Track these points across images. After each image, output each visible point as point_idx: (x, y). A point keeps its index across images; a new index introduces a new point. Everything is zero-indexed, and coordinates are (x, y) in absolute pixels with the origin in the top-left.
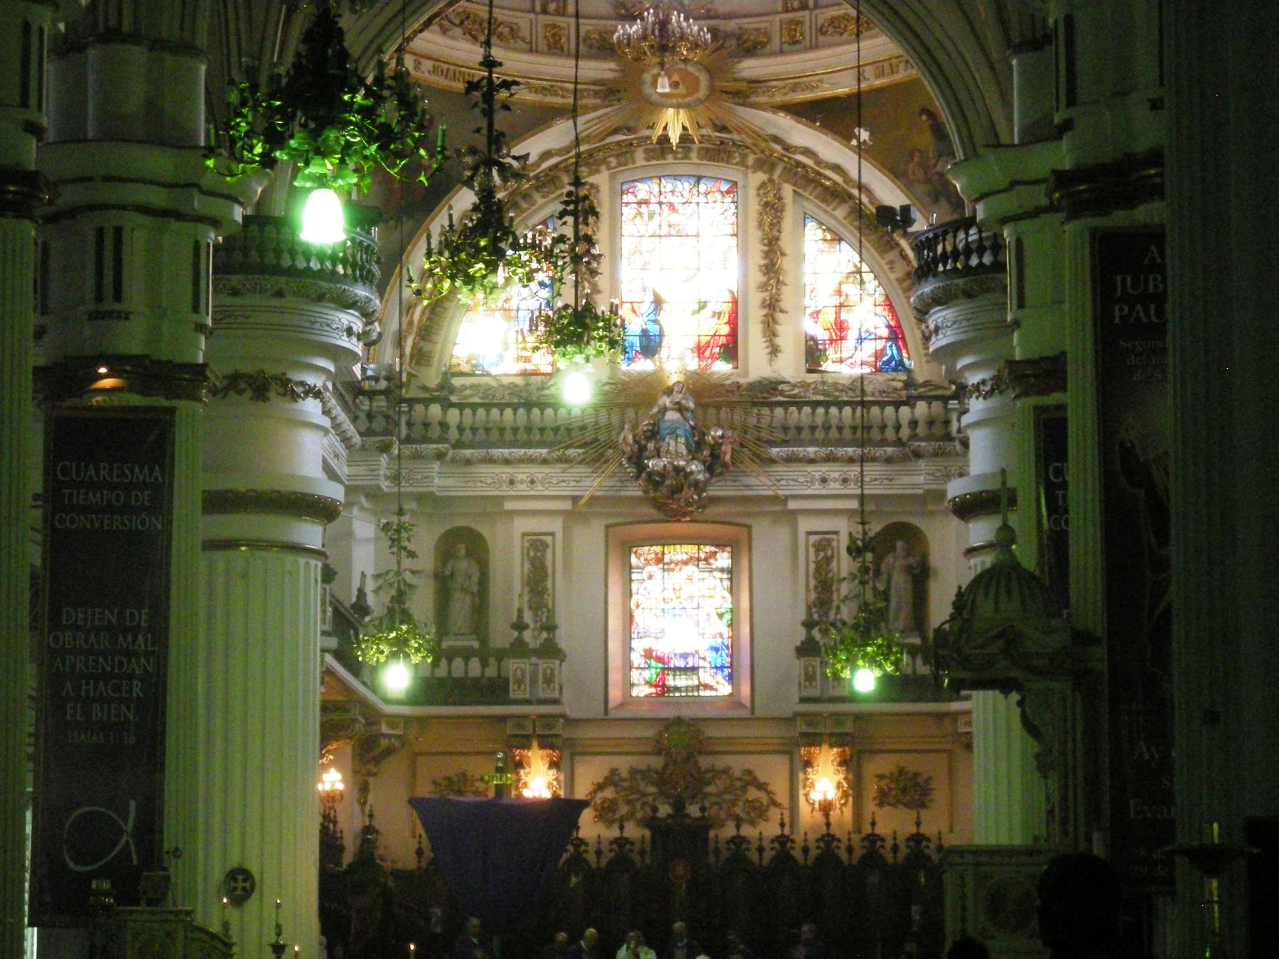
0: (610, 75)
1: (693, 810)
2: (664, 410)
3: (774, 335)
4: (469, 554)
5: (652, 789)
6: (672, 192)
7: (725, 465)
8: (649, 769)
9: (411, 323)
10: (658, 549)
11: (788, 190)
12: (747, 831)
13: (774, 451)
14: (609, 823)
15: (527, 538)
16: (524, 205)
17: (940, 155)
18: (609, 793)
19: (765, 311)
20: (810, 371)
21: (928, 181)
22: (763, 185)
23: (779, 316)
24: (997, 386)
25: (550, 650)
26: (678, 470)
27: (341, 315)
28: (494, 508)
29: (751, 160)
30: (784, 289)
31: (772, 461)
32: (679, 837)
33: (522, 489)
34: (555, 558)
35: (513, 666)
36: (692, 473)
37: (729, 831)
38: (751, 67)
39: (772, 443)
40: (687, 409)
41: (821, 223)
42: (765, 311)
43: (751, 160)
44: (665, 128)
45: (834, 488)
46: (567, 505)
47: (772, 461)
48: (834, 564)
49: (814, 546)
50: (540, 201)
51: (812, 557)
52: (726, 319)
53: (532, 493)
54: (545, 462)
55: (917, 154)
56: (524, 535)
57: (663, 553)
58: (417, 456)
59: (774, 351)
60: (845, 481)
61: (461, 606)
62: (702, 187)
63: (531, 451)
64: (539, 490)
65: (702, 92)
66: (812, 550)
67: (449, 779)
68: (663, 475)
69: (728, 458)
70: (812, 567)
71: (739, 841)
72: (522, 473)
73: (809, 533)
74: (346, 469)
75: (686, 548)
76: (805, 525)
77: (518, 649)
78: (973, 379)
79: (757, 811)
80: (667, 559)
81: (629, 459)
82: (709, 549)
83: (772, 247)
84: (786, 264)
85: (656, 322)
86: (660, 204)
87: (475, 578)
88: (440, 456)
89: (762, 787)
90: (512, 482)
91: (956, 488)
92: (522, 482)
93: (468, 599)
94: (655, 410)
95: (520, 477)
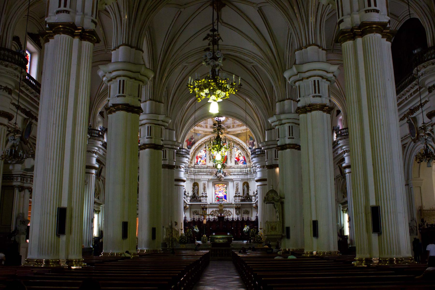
1: (223, 215)
12: (229, 217)
24: (261, 167)
25: (206, 197)
28: (199, 180)
32: (221, 218)
33: (203, 178)
34: (206, 186)
35: (202, 198)
37: (227, 217)
38: (229, 130)
45: (238, 178)
59: (231, 162)
71: (228, 218)
72: (203, 176)
76: (235, 182)
77: (203, 197)
78: (258, 166)
79: (230, 215)
84: (233, 152)
91: (256, 179)
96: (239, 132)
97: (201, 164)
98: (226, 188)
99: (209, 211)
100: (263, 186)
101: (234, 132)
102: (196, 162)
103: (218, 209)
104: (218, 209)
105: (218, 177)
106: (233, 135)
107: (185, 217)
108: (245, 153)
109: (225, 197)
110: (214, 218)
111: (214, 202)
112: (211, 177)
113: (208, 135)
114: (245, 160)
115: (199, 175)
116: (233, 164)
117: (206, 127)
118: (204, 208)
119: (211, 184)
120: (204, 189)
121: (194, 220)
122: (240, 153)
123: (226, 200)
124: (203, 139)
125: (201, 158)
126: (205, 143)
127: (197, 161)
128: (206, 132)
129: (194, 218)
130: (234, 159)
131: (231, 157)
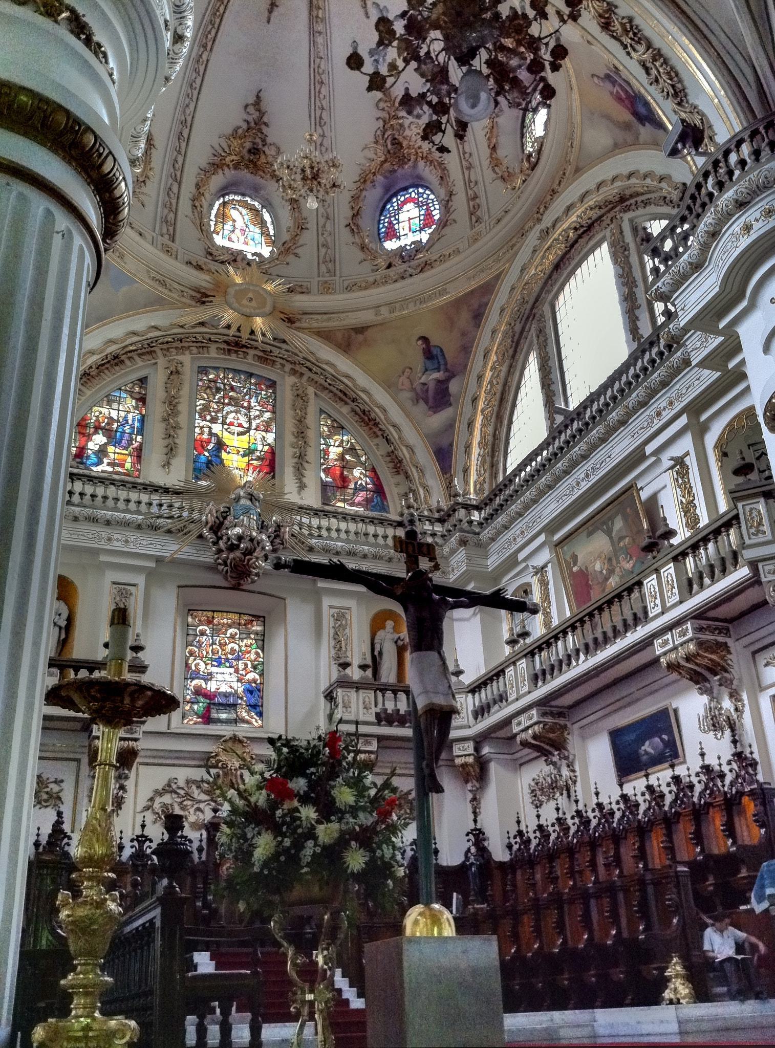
0: (204, 284)
2: (238, 499)
5: (203, 797)
6: (233, 379)
10: (210, 614)
15: (115, 586)
17: (426, 370)
19: (296, 460)
20: (324, 504)
21: (414, 390)
23: (306, 465)
33: (118, 545)
41: (330, 416)
42: (296, 460)
44: (239, 330)
46: (153, 565)
48: (347, 631)
49: (333, 616)
51: (332, 625)
52: (267, 463)
53: (125, 549)
54: (139, 527)
55: (407, 370)
56: (114, 583)
57: (213, 617)
59: (302, 487)
63: (128, 516)
65: (268, 308)
66: (332, 619)
68: (240, 538)
70: (332, 631)
72: (118, 535)
73: (331, 607)
75: (231, 615)
76: (326, 602)
80: (215, 621)
81: (211, 529)
82: (246, 617)
85: (219, 457)
86: (225, 384)
87: (65, 615)
90: (109, 539)
92: (118, 540)
94: (233, 496)
95: (116, 536)
97: (104, 467)
98: (262, 641)
106: (325, 336)
108: (385, 448)
109: (255, 698)
112: (170, 548)
113: (172, 305)
114: (379, 490)
115: (94, 520)
116: (312, 498)
119: (167, 601)
120: (120, 617)
123: (256, 722)
125: (109, 433)
126: (147, 350)
130: (315, 477)
131: (301, 458)
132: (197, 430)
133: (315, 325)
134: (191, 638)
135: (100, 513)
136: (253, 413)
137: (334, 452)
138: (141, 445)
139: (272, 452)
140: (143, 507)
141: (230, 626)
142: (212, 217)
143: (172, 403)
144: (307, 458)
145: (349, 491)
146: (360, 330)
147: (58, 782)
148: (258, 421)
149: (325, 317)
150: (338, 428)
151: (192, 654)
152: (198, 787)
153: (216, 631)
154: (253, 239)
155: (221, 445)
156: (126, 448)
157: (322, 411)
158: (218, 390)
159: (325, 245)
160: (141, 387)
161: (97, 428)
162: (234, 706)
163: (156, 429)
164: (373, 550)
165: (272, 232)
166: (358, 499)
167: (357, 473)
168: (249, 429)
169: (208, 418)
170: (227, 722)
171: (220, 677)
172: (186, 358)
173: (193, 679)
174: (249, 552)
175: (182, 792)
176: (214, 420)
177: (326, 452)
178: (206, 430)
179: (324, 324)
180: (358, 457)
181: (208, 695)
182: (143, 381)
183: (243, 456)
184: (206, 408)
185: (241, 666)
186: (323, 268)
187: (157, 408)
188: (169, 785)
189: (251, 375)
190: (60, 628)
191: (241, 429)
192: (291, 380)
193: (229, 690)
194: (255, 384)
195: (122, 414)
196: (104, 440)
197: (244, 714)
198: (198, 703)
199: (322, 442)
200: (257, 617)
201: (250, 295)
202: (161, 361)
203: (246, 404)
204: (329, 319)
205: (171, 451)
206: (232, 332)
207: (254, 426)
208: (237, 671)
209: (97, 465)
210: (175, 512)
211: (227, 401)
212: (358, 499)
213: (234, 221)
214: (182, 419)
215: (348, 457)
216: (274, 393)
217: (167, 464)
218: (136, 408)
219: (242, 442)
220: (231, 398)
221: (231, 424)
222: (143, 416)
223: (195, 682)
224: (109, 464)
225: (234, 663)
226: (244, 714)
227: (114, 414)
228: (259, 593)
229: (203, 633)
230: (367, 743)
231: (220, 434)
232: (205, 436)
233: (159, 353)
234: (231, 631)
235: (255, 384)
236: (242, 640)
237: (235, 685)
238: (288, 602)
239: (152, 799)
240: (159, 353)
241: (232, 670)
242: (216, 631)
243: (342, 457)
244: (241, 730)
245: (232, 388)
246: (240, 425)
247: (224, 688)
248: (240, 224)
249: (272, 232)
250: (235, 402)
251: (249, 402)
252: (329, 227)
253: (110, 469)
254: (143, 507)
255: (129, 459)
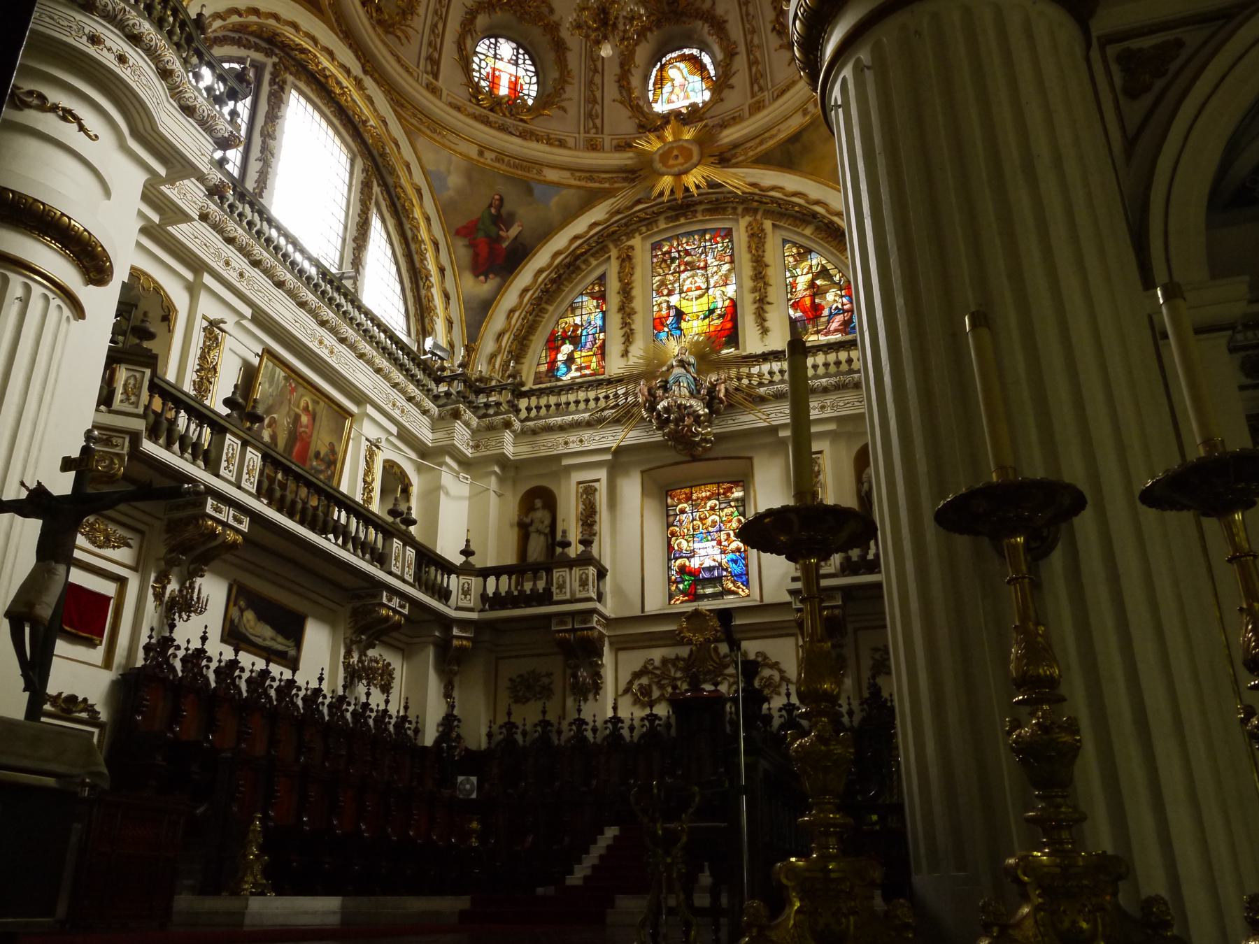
0: (629, 162)
3: (764, 320)
4: (545, 507)
5: (679, 675)
6: (687, 243)
7: (721, 401)
8: (678, 658)
9: (500, 347)
10: (687, 490)
11: (768, 224)
13: (762, 390)
14: (643, 706)
16: (584, 267)
18: (644, 681)
22: (750, 224)
23: (767, 307)
26: (679, 406)
27: (79, 17)
29: (740, 210)
30: (769, 289)
31: (763, 400)
36: (691, 406)
39: (761, 384)
40: (689, 364)
41: (795, 244)
43: (740, 210)
44: (672, 192)
46: (609, 457)
47: (763, 400)
50: (594, 263)
54: (589, 424)
56: (579, 483)
58: (491, 428)
59: (765, 331)
60: (823, 407)
61: (536, 548)
62: (707, 237)
63: (576, 417)
64: (587, 446)
65: (695, 159)
67: (521, 676)
69: (722, 395)
72: (573, 437)
74: (430, 436)
75: (709, 487)
80: (694, 496)
82: (726, 486)
83: (759, 265)
87: (547, 522)
88: (508, 425)
89: (775, 666)
90: (566, 443)
93: (542, 538)
94: (664, 369)
96: (796, 122)
97: (574, 374)
99: (615, 670)
100: (886, 34)
101: (759, 136)
102: (543, 368)
103: (684, 652)
104: (684, 652)
105: (662, 423)
106: (764, 161)
107: (449, 722)
110: (652, 718)
111: (655, 602)
115: (549, 429)
117: (593, 147)
118: (579, 648)
119: (631, 488)
121: (509, 741)
122: (824, 273)
124: (580, 226)
125: (575, 340)
127: (553, 364)
128: (591, 173)
129: (510, 726)
132: (656, 308)
133: (751, 153)
134: (671, 519)
135: (552, 421)
136: (710, 270)
137: (803, 281)
138: (604, 341)
139: (734, 303)
140: (592, 404)
141: (709, 498)
142: (651, 87)
143: (626, 292)
144: (769, 299)
145: (823, 319)
146: (795, 138)
147: (549, 675)
148: (716, 277)
149: (758, 140)
150: (804, 253)
151: (673, 534)
152: (674, 665)
153: (695, 506)
154: (693, 90)
155: (680, 315)
156: (591, 349)
157: (785, 241)
158: (673, 260)
159: (756, 62)
160: (600, 286)
161: (565, 338)
162: (720, 578)
163: (615, 320)
164: (833, 380)
165: (712, 73)
166: (834, 326)
167: (830, 296)
168: (708, 289)
169: (665, 292)
170: (714, 596)
171: (702, 552)
172: (636, 242)
173: (676, 559)
174: (680, 420)
175: (658, 672)
176: (670, 294)
177: (793, 285)
178: (664, 305)
179: (759, 149)
180: (830, 277)
181: (694, 573)
182: (602, 279)
183: (705, 318)
184: (663, 283)
185: (723, 537)
186: (756, 88)
187: (614, 300)
188: (645, 667)
189: (705, 232)
190: (546, 535)
191: (699, 292)
192: (744, 222)
193: (713, 564)
194: (710, 240)
195: (585, 317)
196: (571, 348)
197: (730, 585)
198: (682, 581)
199: (788, 274)
200: (736, 483)
201: (675, 152)
202: (614, 253)
203: (702, 264)
204: (761, 143)
205: (628, 338)
206: (665, 198)
207: (712, 284)
208: (719, 543)
209: (566, 374)
210: (621, 401)
211: (682, 268)
212: (834, 326)
213: (673, 80)
214: (637, 304)
215: (819, 282)
216: (731, 241)
217: (625, 354)
218: (597, 307)
219: (701, 306)
220: (687, 264)
221: (689, 290)
222: (604, 313)
223: (679, 561)
224: (577, 370)
225: (716, 535)
226: (730, 585)
227: (578, 320)
228: (723, 458)
229: (683, 511)
230: (831, 598)
231: (678, 305)
232: (664, 312)
233: (611, 246)
234: (710, 503)
235: (710, 240)
236: (722, 509)
237: (718, 558)
238: (756, 461)
239: (630, 683)
240: (611, 246)
241: (714, 543)
242: (695, 506)
243: (812, 285)
244: (729, 602)
245: (687, 253)
246: (699, 288)
247: (708, 563)
248: (679, 80)
249: (712, 73)
250: (692, 266)
251: (706, 261)
252: (756, 41)
253: (578, 374)
254: (592, 404)
255: (594, 359)
